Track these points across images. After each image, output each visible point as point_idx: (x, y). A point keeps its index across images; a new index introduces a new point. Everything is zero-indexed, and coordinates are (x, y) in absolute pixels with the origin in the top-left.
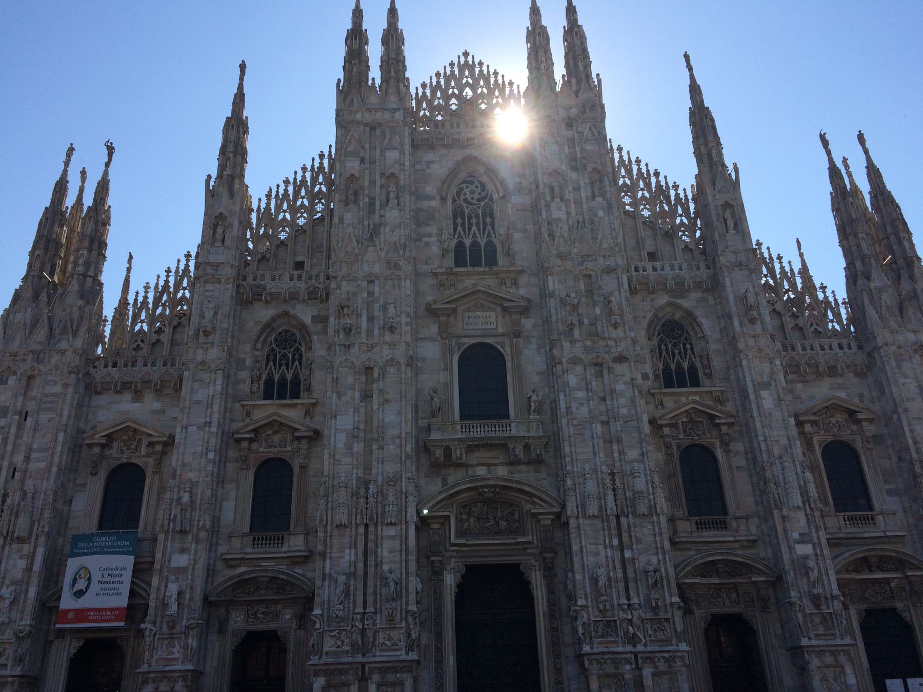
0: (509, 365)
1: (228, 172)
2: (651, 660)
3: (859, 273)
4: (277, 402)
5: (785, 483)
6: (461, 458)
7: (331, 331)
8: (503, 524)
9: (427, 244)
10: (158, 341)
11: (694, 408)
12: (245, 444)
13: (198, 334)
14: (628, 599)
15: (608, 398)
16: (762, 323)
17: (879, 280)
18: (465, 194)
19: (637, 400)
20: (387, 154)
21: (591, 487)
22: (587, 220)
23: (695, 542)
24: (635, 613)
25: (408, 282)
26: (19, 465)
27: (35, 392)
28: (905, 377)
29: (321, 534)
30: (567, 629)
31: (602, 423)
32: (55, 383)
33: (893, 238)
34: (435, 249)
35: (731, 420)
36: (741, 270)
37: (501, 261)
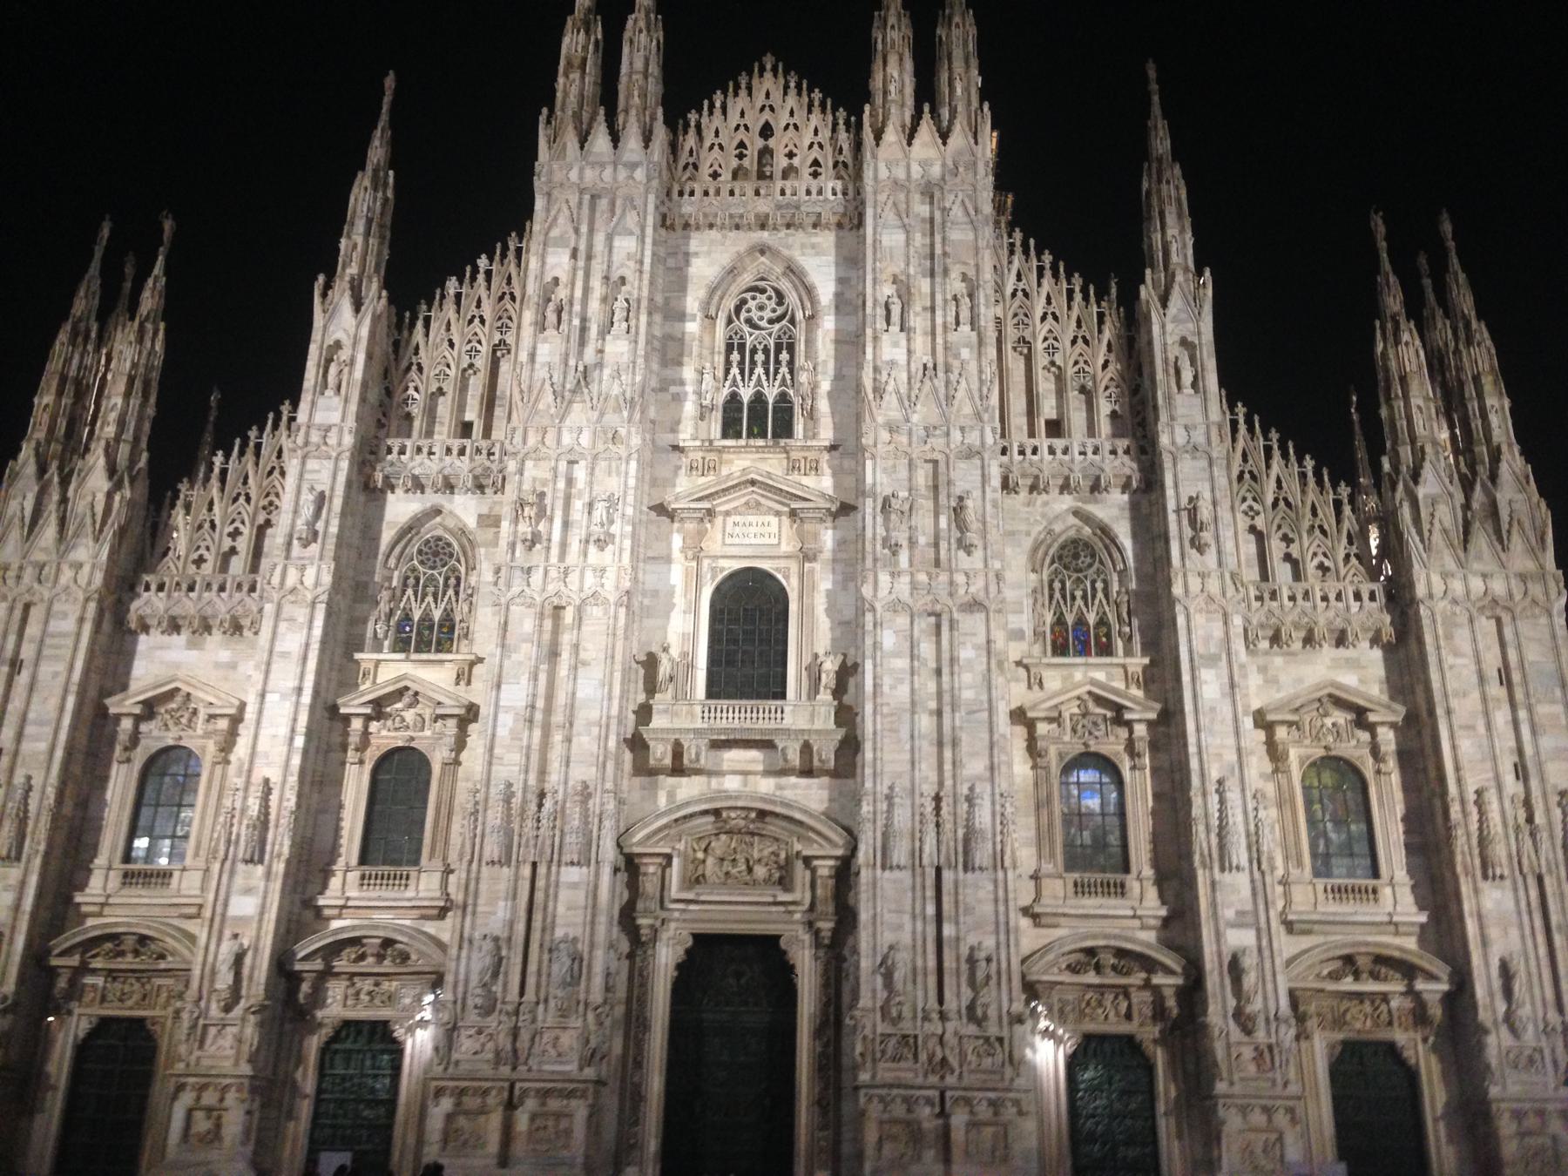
0: (793, 607)
1: (353, 270)
2: (968, 1102)
3: (1404, 469)
4: (414, 656)
5: (1221, 827)
6: (698, 760)
7: (503, 543)
8: (760, 872)
10: (233, 551)
11: (1090, 693)
13: (289, 544)
14: (941, 1001)
15: (946, 670)
16: (1219, 552)
18: (749, 311)
19: (994, 676)
20: (617, 242)
21: (902, 817)
22: (940, 368)
23: (1065, 915)
24: (950, 1026)
25: (633, 465)
27: (33, 629)
28: (1456, 654)
30: (845, 1043)
31: (931, 713)
32: (65, 615)
33: (1473, 406)
34: (690, 408)
35: (1153, 716)
36: (1194, 458)
37: (799, 428)
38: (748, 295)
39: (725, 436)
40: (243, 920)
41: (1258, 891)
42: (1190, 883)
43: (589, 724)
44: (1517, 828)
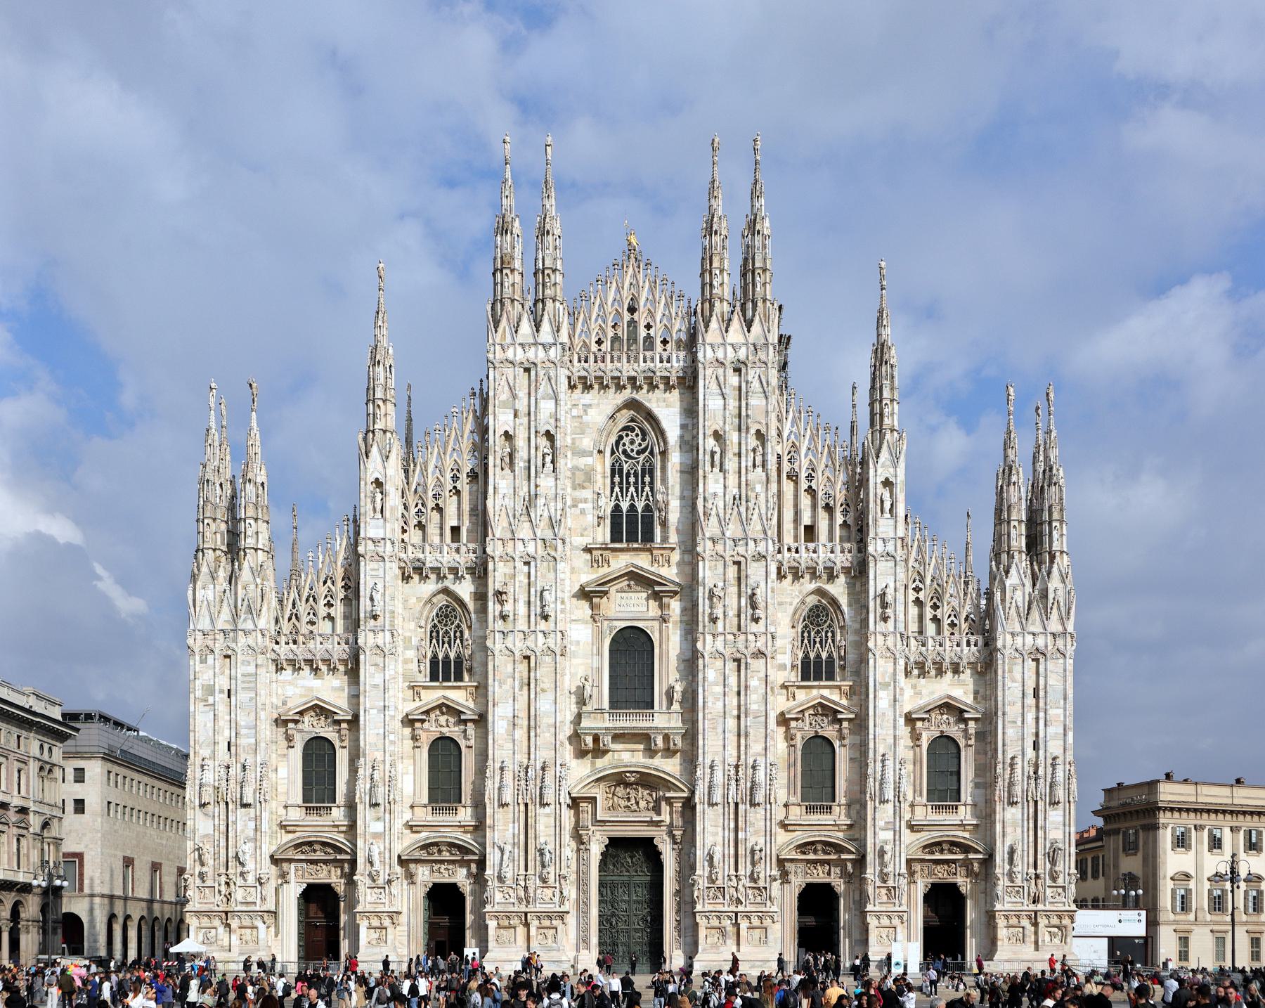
0: (657, 651)
9: (583, 512)
12: (418, 725)
14: (737, 870)
15: (743, 693)
17: (1017, 581)
21: (719, 777)
26: (233, 740)
28: (1014, 681)
29: (489, 811)
34: (591, 519)
35: (852, 716)
38: (624, 434)
39: (613, 541)
40: (376, 836)
41: (897, 812)
42: (864, 806)
43: (549, 726)
44: (1029, 777)
